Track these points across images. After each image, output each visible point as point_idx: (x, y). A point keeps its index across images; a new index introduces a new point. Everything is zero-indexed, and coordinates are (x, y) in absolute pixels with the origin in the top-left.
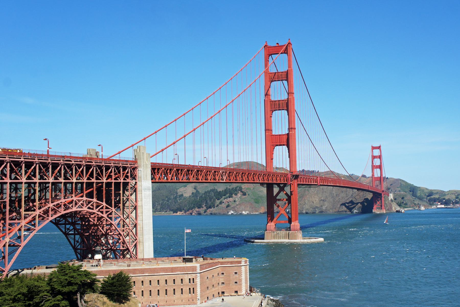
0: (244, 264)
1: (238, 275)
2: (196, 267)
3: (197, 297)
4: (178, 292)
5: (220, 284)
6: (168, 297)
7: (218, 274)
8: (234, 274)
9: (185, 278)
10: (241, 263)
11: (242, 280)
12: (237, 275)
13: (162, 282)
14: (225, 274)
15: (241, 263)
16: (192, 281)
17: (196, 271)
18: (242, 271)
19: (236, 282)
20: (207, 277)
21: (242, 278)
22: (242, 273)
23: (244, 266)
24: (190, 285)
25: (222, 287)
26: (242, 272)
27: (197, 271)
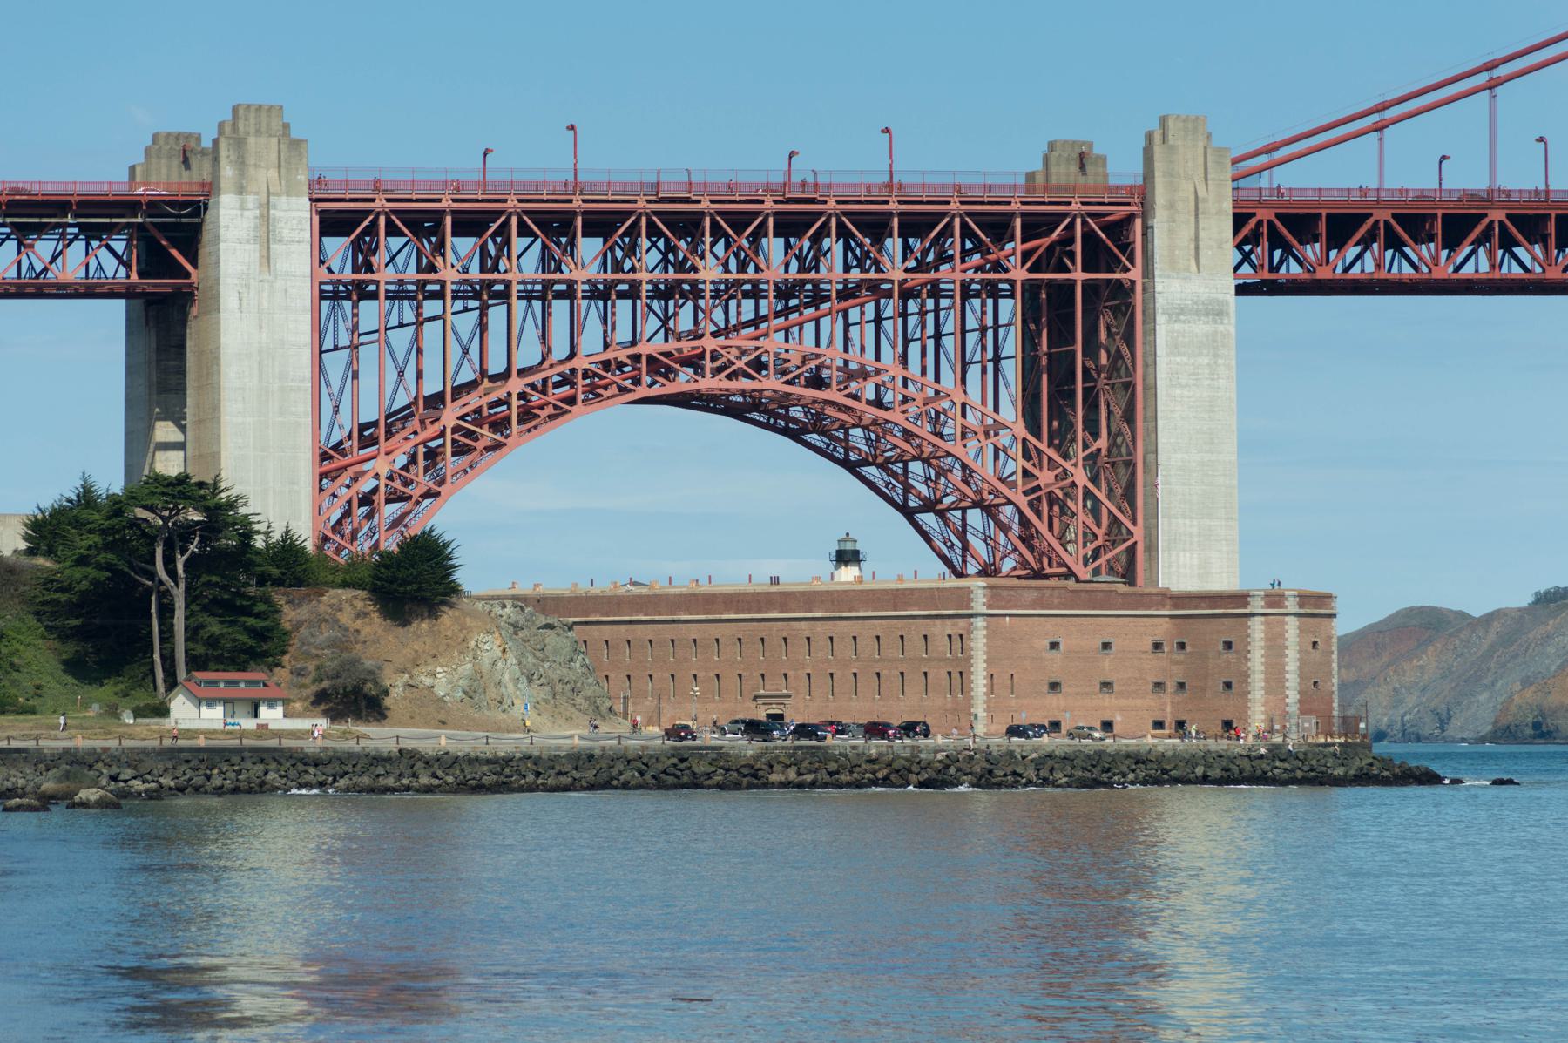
0: (1262, 607)
1: (1237, 652)
2: (969, 591)
3: (972, 710)
4: (915, 683)
5: (1171, 686)
6: (881, 703)
7: (1157, 646)
8: (1221, 647)
9: (936, 632)
10: (1248, 603)
11: (1249, 676)
12: (1231, 657)
13: (867, 644)
14: (1188, 649)
15: (1246, 604)
16: (957, 644)
17: (969, 607)
18: (1248, 636)
19: (1228, 685)
20: (1054, 646)
21: (1249, 669)
22: (1249, 648)
23: (1262, 618)
24: (948, 659)
25: (1178, 703)
26: (1249, 640)
27: (972, 608)
